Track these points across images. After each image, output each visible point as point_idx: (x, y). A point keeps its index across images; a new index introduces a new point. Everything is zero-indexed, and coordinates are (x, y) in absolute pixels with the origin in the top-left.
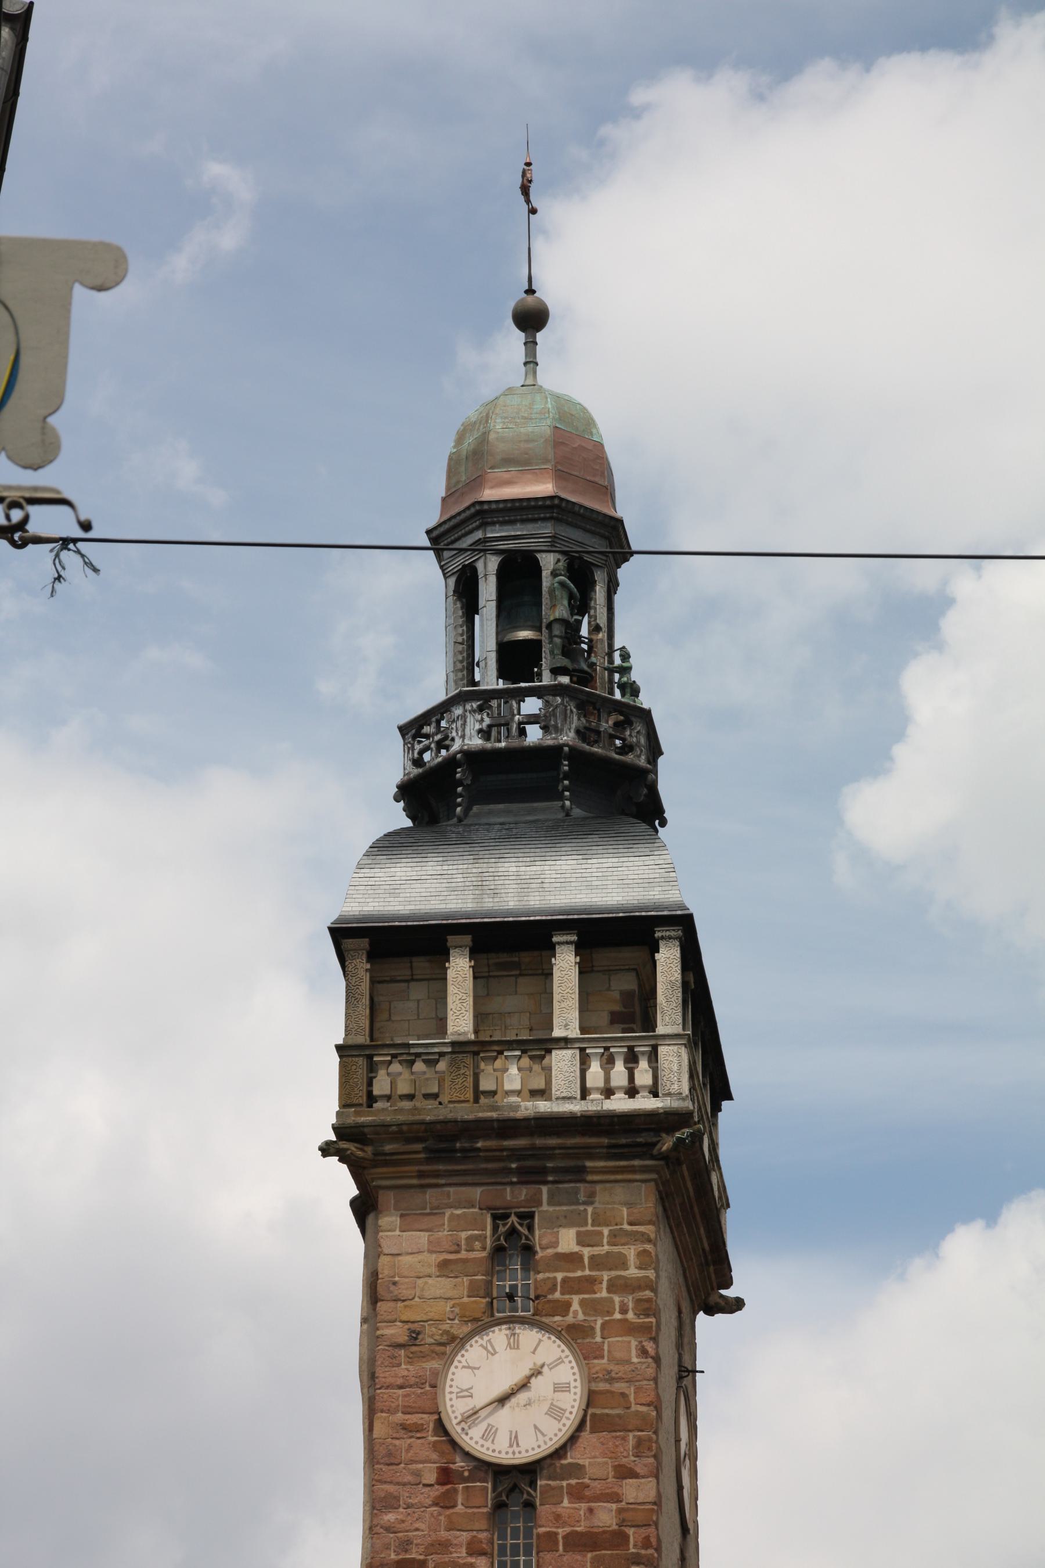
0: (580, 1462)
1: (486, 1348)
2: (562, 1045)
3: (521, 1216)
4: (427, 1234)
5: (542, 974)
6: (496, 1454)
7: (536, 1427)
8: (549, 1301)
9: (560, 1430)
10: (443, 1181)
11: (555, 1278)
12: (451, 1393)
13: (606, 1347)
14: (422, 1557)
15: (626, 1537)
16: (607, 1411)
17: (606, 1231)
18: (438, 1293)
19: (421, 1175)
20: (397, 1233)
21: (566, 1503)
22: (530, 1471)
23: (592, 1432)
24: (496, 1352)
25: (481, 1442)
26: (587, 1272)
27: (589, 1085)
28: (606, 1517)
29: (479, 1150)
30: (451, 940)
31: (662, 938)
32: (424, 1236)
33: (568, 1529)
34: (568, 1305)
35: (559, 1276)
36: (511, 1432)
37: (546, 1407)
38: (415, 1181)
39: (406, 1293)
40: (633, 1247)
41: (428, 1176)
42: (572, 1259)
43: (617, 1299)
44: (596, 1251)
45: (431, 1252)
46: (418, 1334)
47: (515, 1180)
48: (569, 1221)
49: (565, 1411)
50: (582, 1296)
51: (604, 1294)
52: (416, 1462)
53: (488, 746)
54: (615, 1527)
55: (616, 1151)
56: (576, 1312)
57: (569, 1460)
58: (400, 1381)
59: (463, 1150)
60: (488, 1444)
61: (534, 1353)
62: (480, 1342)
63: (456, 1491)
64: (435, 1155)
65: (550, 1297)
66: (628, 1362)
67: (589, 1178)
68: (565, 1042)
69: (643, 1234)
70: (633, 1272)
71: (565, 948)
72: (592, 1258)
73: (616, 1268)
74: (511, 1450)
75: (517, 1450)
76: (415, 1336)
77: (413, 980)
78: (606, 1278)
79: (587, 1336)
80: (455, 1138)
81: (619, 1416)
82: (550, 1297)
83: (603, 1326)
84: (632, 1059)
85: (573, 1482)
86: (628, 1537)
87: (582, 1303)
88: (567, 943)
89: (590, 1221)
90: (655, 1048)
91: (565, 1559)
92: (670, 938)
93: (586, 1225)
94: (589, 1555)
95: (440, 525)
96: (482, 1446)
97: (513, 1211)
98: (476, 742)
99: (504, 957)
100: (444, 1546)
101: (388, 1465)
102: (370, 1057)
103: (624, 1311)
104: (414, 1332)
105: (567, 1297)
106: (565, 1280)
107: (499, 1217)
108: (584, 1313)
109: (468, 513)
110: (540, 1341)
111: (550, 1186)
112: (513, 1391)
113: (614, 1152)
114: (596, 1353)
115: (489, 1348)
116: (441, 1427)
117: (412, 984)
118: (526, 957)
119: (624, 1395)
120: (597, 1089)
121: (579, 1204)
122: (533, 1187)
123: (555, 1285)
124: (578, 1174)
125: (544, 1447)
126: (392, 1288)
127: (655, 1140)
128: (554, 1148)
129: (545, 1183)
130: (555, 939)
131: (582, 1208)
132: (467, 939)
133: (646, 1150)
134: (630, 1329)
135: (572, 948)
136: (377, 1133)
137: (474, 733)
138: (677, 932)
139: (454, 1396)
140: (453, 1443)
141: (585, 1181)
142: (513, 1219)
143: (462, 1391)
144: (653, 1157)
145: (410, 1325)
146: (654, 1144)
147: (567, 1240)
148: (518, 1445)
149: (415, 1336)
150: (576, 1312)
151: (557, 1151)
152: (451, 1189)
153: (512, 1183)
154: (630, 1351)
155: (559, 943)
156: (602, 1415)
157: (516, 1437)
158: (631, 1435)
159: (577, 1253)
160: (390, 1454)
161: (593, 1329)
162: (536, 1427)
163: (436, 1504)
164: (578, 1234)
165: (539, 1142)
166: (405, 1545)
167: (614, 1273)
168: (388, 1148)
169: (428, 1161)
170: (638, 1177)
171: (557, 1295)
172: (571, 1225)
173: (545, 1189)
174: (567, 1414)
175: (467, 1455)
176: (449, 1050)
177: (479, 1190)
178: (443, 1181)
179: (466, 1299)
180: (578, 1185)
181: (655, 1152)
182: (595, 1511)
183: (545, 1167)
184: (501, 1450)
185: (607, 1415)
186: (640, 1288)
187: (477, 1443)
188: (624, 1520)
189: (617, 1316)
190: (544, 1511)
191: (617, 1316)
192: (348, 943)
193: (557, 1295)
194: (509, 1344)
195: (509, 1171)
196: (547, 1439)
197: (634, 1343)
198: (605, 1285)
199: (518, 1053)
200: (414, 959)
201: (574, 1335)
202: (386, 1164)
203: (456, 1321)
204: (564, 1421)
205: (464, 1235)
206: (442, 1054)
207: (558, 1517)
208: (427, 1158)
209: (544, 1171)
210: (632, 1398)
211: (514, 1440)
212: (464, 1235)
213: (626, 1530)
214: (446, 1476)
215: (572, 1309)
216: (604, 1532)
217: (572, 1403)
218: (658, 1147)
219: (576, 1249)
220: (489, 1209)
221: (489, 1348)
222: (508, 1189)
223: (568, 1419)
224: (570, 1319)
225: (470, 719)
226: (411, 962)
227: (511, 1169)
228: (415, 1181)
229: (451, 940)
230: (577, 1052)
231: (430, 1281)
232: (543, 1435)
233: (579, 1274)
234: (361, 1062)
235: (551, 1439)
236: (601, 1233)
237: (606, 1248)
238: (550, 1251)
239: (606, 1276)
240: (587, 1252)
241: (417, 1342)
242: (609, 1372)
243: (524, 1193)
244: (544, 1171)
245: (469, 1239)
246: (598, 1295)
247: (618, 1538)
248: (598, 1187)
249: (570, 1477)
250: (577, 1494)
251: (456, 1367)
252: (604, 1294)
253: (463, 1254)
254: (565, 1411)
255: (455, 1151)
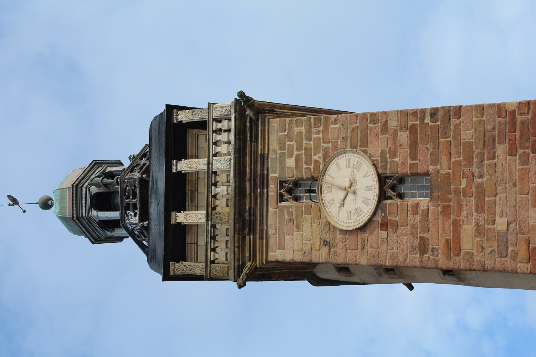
0: (380, 152)
1: (331, 204)
2: (210, 166)
3: (282, 187)
4: (286, 236)
5: (198, 180)
6: (375, 198)
7: (364, 177)
8: (314, 171)
9: (366, 163)
10: (265, 227)
11: (305, 168)
12: (349, 223)
13: (333, 141)
14: (419, 239)
15: (413, 125)
16: (359, 139)
17: (288, 143)
18: (309, 230)
19: (261, 238)
20: (285, 251)
21: (397, 159)
22: (382, 180)
23: (367, 146)
24: (333, 199)
25: (370, 206)
26: (303, 152)
27: (226, 152)
28: (404, 137)
29: (250, 208)
30: (173, 222)
31: (177, 119)
32: (287, 237)
33: (408, 158)
34: (316, 161)
35: (305, 166)
36: (366, 190)
37: (356, 171)
38: (265, 241)
39: (308, 248)
40: (295, 129)
41: (263, 235)
42: (298, 160)
43: (314, 136)
44: (295, 148)
45: (293, 235)
46: (325, 240)
47: (266, 190)
48: (282, 162)
49: (358, 161)
50: (312, 155)
51: (312, 142)
52: (378, 242)
53: (137, 211)
54: (408, 132)
55: (253, 138)
56: (319, 157)
57: (379, 158)
58: (344, 250)
59: (250, 216)
60: (370, 202)
61: (334, 179)
62: (328, 207)
63: (390, 220)
64: (252, 230)
65: (312, 171)
66: (339, 129)
67: (266, 152)
68: (208, 164)
69: (289, 124)
70: (303, 129)
71: (179, 166)
72: (298, 150)
73: (302, 137)
74: (374, 190)
75: (374, 187)
76: (326, 243)
77: (197, 244)
78: (306, 142)
79: (328, 151)
80: (244, 220)
81: (361, 132)
82: (312, 171)
83: (325, 142)
84: (218, 131)
85: (388, 156)
86: (412, 124)
87: (315, 155)
88: (177, 165)
89: (283, 151)
90: (214, 120)
91: (421, 159)
92: (177, 115)
93: (285, 153)
94: (420, 145)
95: (88, 238)
96: (371, 205)
97: (279, 191)
98: (137, 218)
99: (188, 198)
100: (413, 226)
101: (378, 258)
102: (213, 262)
103: (318, 132)
104: (324, 242)
105: (312, 162)
106: (306, 164)
107: (282, 198)
108: (320, 152)
109: (79, 224)
110: (329, 175)
111: (270, 172)
112: (350, 190)
113: (255, 138)
114: (335, 146)
115: (331, 202)
116: (363, 228)
117: (199, 244)
118: (189, 188)
119: (353, 130)
120: (228, 147)
121: (277, 157)
122: (270, 182)
123: (308, 168)
124: (264, 158)
125: (373, 173)
126: (306, 254)
127: (249, 118)
128: (251, 169)
129: (268, 175)
130: (174, 171)
131: (278, 155)
132: (173, 213)
133: (254, 123)
134: (326, 127)
135: (179, 162)
136: (239, 260)
137: (135, 218)
138: (174, 111)
139: (350, 221)
140: (370, 221)
141: (268, 154)
142: (282, 191)
143: (348, 217)
144: (258, 120)
145: (322, 245)
146: (251, 119)
147: (290, 162)
148: (371, 186)
149: (326, 243)
150: (319, 157)
151: (252, 168)
152: (269, 223)
153: (267, 192)
154: (335, 128)
155: (176, 169)
156: (360, 141)
157: (368, 187)
158: (369, 125)
159: (295, 158)
160: (374, 256)
161: (325, 148)
162: (364, 177)
163: (396, 232)
164: (288, 157)
165: (248, 176)
166: (413, 248)
167: (304, 138)
168: (247, 255)
169: (255, 234)
170: (267, 128)
171: (312, 167)
172: (284, 161)
173: (271, 175)
174: (359, 160)
175: (374, 214)
176: (210, 222)
177: (271, 210)
178: (265, 227)
179: (312, 215)
180: (270, 158)
181: (254, 118)
182: (401, 143)
183: (260, 174)
184: (373, 195)
185: (361, 138)
186: (310, 124)
187: (370, 209)
188: (405, 127)
189: (320, 136)
190: (400, 171)
191: (320, 136)
192: (171, 273)
193: (312, 167)
194: (330, 192)
195: (262, 194)
196: (369, 170)
197: (332, 126)
198: (308, 142)
199: (213, 187)
200: (187, 242)
201: (328, 159)
202: (255, 256)
203: (321, 221)
204: (362, 161)
205: (287, 217)
206: (212, 226)
207: (403, 163)
208: (253, 235)
209: (262, 175)
210: (354, 126)
211: (369, 188)
212: (287, 217)
213: (409, 125)
214: (384, 226)
215: (317, 159)
216: (410, 137)
217: (354, 158)
218: (252, 117)
219: (294, 158)
220: (277, 204)
221: (331, 202)
222: (270, 194)
223: (361, 159)
224: (321, 160)
225: (131, 221)
226: (188, 244)
227: (260, 192)
228: (265, 241)
229: (173, 222)
230: (214, 158)
231: (304, 234)
232: (368, 172)
233: (303, 156)
234: (213, 266)
235: (370, 168)
236: (288, 145)
237: (294, 142)
238: (294, 171)
239: (305, 142)
240: (295, 153)
241: (328, 241)
242: (343, 138)
243: (272, 186)
244: (262, 175)
245: (288, 214)
246: (312, 146)
247: (413, 130)
248: (271, 148)
249: (386, 157)
250: (394, 154)
251: (339, 220)
252: (312, 142)
253: (294, 217)
254: (358, 161)
255: (250, 220)
